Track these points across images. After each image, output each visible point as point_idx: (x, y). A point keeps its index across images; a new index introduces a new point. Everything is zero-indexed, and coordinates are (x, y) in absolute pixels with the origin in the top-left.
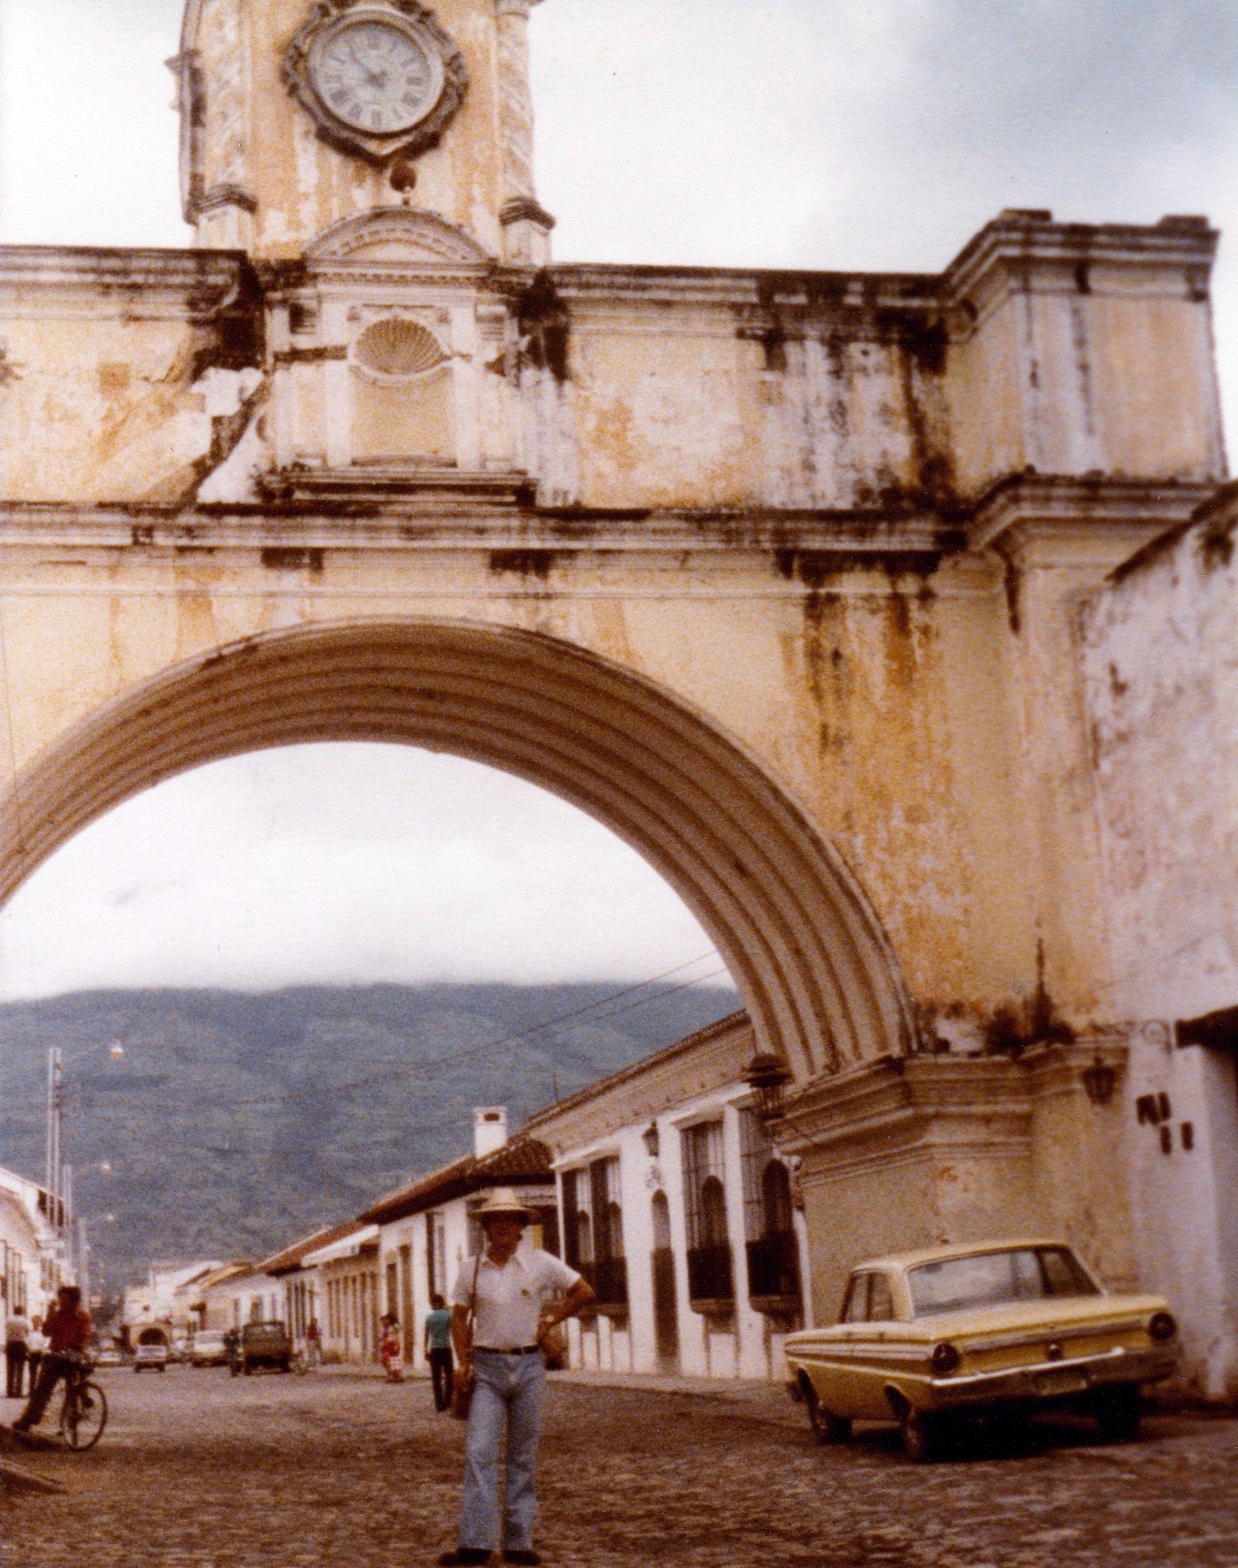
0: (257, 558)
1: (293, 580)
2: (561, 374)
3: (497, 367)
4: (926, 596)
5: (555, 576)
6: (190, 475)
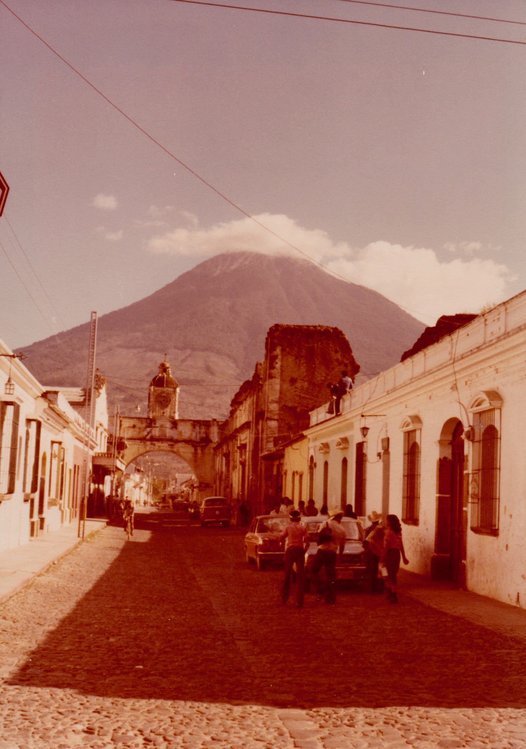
1: (152, 446)
2: (176, 429)
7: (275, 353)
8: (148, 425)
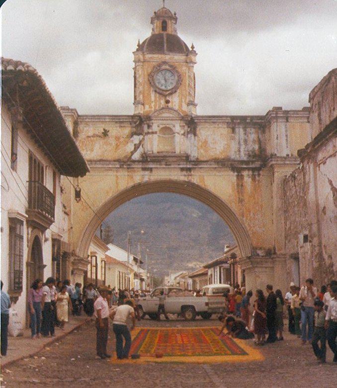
0: (140, 169)
1: (147, 173)
2: (195, 135)
3: (184, 134)
4: (259, 175)
5: (192, 173)
6: (130, 154)
8: (134, 130)
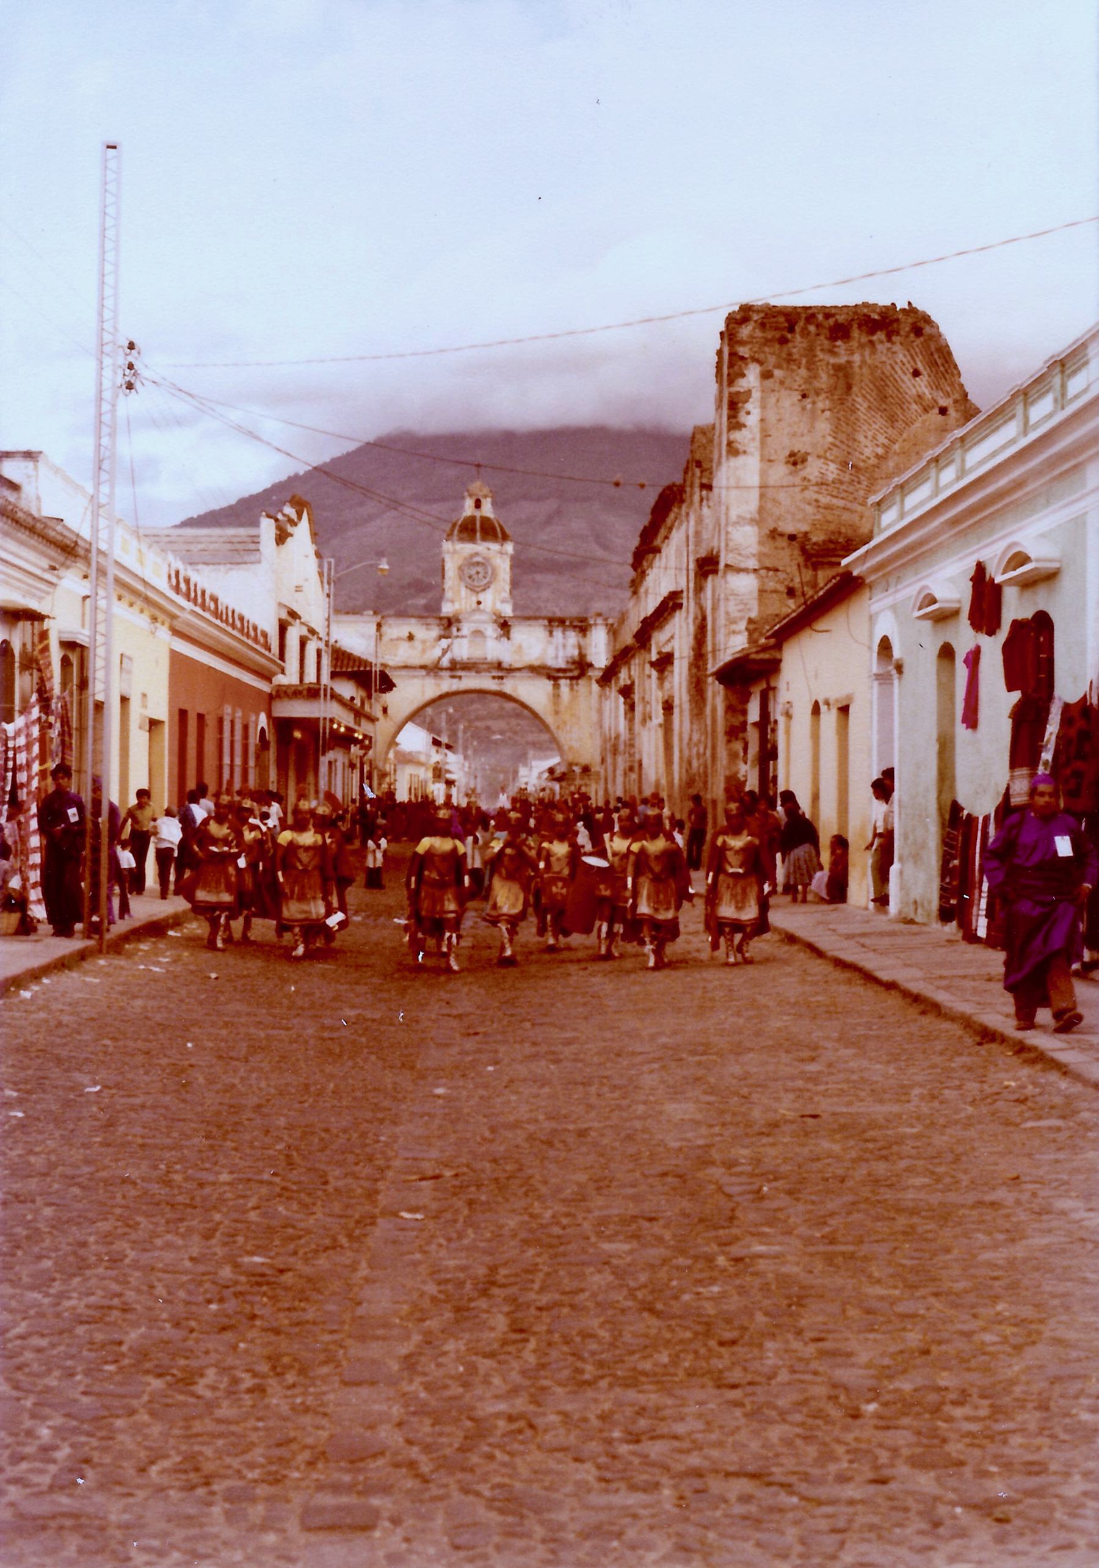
1: (456, 681)
7: (742, 384)
